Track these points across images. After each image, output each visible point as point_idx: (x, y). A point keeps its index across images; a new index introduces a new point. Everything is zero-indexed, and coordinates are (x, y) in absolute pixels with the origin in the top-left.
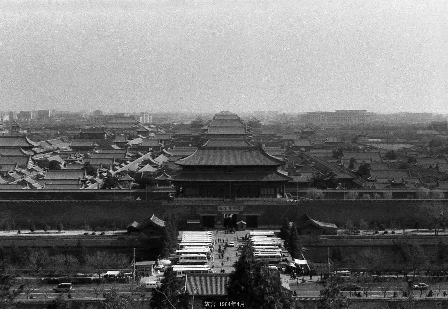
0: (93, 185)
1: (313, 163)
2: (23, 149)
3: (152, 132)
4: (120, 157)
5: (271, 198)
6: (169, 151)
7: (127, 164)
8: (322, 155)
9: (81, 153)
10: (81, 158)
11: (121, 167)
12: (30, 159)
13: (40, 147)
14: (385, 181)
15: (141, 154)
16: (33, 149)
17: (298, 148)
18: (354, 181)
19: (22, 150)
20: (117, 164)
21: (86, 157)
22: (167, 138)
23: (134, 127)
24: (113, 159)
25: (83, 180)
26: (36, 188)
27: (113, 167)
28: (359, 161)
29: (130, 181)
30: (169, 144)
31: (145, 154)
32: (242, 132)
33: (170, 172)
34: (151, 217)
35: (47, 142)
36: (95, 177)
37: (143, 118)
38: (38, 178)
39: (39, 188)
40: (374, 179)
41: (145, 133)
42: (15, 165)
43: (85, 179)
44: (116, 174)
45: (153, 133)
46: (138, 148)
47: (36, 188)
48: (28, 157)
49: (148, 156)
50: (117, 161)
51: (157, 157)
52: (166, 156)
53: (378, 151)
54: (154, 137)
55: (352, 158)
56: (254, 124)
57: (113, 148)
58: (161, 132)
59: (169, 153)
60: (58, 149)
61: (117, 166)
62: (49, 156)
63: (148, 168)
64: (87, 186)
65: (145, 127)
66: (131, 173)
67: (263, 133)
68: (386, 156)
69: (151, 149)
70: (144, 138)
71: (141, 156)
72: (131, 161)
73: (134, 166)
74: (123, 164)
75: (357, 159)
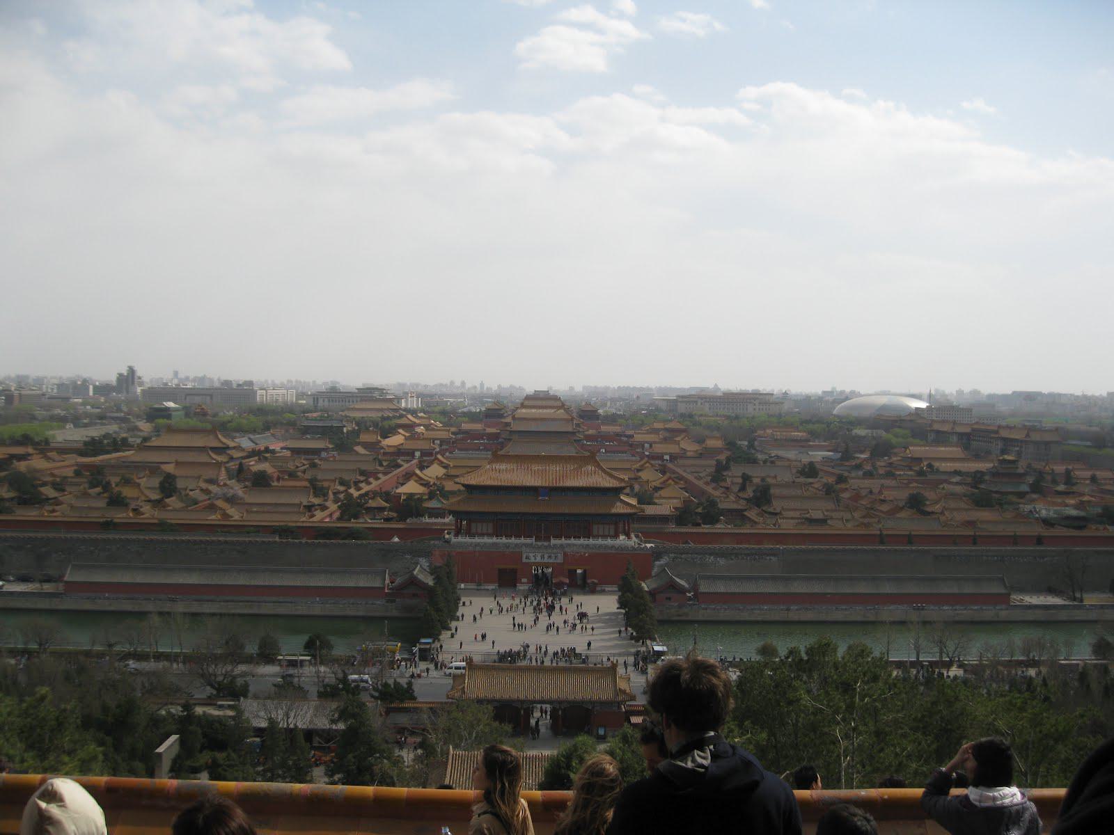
0: (322, 513)
1: (682, 482)
2: (212, 451)
3: (421, 425)
5: (609, 540)
6: (447, 458)
7: (377, 479)
9: (304, 459)
10: (305, 467)
11: (369, 483)
12: (223, 469)
14: (797, 514)
15: (402, 463)
16: (229, 452)
17: (660, 457)
18: (746, 513)
19: (210, 453)
20: (362, 478)
21: (313, 465)
22: (444, 435)
23: (391, 415)
25: (308, 504)
26: (232, 517)
28: (756, 481)
29: (382, 509)
31: (408, 461)
33: (445, 494)
34: (414, 570)
35: (250, 439)
36: (326, 500)
37: (407, 402)
38: (232, 500)
39: (236, 517)
40: (778, 510)
41: (409, 427)
43: (310, 504)
44: (361, 496)
45: (422, 427)
46: (400, 452)
47: (232, 517)
48: (219, 464)
50: (362, 473)
51: (428, 467)
52: (442, 467)
53: (787, 464)
54: (423, 434)
55: (744, 474)
56: (588, 414)
57: (355, 451)
58: (436, 426)
59: (445, 461)
61: (362, 482)
62: (252, 463)
63: (412, 487)
64: (313, 516)
65: (410, 416)
66: (387, 496)
67: (604, 428)
69: (418, 454)
70: (407, 435)
71: (400, 466)
72: (385, 474)
74: (371, 480)
75: (753, 477)
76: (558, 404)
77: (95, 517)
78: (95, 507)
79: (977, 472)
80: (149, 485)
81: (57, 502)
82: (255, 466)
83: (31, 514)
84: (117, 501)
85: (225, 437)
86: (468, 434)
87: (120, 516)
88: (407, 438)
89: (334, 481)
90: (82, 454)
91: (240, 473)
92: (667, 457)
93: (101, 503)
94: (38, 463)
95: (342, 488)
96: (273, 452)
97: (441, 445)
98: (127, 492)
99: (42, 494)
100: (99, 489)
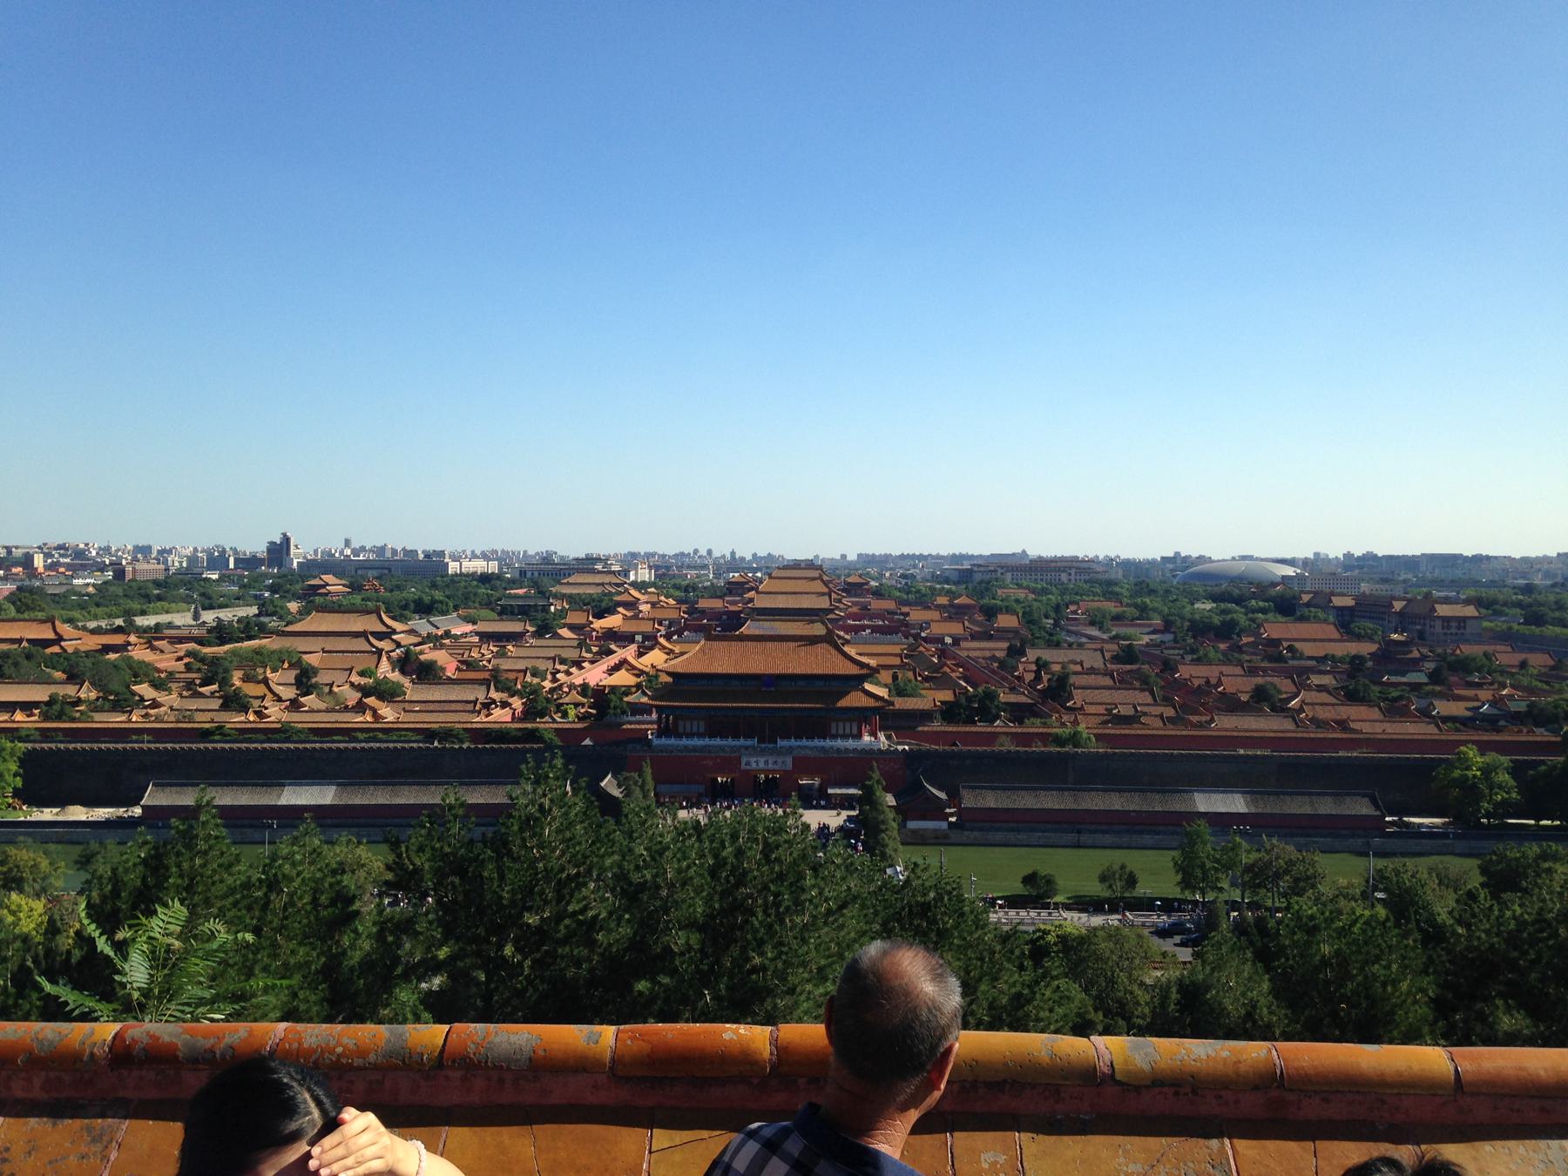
4: (572, 654)
8: (988, 654)
13: (412, 632)
17: (940, 640)
20: (563, 668)
22: (673, 615)
24: (554, 659)
27: (554, 674)
30: (675, 630)
32: (824, 603)
42: (351, 670)
46: (611, 635)
48: (379, 652)
49: (629, 653)
50: (563, 662)
60: (447, 634)
65: (633, 592)
68: (1113, 657)
69: (639, 638)
72: (592, 662)
73: (595, 675)
76: (816, 574)
77: (203, 721)
78: (206, 710)
79: (1355, 657)
80: (282, 681)
81: (155, 704)
82: (429, 654)
83: (116, 720)
84: (233, 702)
85: (394, 618)
86: (703, 612)
87: (236, 719)
88: (625, 618)
89: (525, 672)
90: (201, 641)
91: (406, 663)
92: (948, 640)
93: (215, 704)
94: (140, 654)
95: (536, 680)
96: (456, 637)
97: (670, 626)
98: (252, 689)
99: (134, 694)
100: (215, 687)
